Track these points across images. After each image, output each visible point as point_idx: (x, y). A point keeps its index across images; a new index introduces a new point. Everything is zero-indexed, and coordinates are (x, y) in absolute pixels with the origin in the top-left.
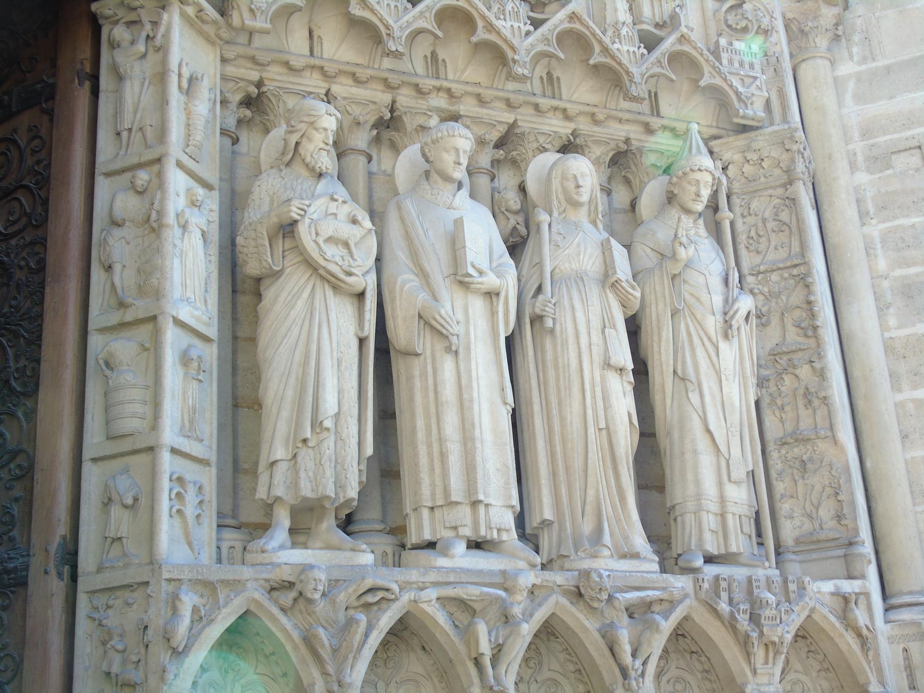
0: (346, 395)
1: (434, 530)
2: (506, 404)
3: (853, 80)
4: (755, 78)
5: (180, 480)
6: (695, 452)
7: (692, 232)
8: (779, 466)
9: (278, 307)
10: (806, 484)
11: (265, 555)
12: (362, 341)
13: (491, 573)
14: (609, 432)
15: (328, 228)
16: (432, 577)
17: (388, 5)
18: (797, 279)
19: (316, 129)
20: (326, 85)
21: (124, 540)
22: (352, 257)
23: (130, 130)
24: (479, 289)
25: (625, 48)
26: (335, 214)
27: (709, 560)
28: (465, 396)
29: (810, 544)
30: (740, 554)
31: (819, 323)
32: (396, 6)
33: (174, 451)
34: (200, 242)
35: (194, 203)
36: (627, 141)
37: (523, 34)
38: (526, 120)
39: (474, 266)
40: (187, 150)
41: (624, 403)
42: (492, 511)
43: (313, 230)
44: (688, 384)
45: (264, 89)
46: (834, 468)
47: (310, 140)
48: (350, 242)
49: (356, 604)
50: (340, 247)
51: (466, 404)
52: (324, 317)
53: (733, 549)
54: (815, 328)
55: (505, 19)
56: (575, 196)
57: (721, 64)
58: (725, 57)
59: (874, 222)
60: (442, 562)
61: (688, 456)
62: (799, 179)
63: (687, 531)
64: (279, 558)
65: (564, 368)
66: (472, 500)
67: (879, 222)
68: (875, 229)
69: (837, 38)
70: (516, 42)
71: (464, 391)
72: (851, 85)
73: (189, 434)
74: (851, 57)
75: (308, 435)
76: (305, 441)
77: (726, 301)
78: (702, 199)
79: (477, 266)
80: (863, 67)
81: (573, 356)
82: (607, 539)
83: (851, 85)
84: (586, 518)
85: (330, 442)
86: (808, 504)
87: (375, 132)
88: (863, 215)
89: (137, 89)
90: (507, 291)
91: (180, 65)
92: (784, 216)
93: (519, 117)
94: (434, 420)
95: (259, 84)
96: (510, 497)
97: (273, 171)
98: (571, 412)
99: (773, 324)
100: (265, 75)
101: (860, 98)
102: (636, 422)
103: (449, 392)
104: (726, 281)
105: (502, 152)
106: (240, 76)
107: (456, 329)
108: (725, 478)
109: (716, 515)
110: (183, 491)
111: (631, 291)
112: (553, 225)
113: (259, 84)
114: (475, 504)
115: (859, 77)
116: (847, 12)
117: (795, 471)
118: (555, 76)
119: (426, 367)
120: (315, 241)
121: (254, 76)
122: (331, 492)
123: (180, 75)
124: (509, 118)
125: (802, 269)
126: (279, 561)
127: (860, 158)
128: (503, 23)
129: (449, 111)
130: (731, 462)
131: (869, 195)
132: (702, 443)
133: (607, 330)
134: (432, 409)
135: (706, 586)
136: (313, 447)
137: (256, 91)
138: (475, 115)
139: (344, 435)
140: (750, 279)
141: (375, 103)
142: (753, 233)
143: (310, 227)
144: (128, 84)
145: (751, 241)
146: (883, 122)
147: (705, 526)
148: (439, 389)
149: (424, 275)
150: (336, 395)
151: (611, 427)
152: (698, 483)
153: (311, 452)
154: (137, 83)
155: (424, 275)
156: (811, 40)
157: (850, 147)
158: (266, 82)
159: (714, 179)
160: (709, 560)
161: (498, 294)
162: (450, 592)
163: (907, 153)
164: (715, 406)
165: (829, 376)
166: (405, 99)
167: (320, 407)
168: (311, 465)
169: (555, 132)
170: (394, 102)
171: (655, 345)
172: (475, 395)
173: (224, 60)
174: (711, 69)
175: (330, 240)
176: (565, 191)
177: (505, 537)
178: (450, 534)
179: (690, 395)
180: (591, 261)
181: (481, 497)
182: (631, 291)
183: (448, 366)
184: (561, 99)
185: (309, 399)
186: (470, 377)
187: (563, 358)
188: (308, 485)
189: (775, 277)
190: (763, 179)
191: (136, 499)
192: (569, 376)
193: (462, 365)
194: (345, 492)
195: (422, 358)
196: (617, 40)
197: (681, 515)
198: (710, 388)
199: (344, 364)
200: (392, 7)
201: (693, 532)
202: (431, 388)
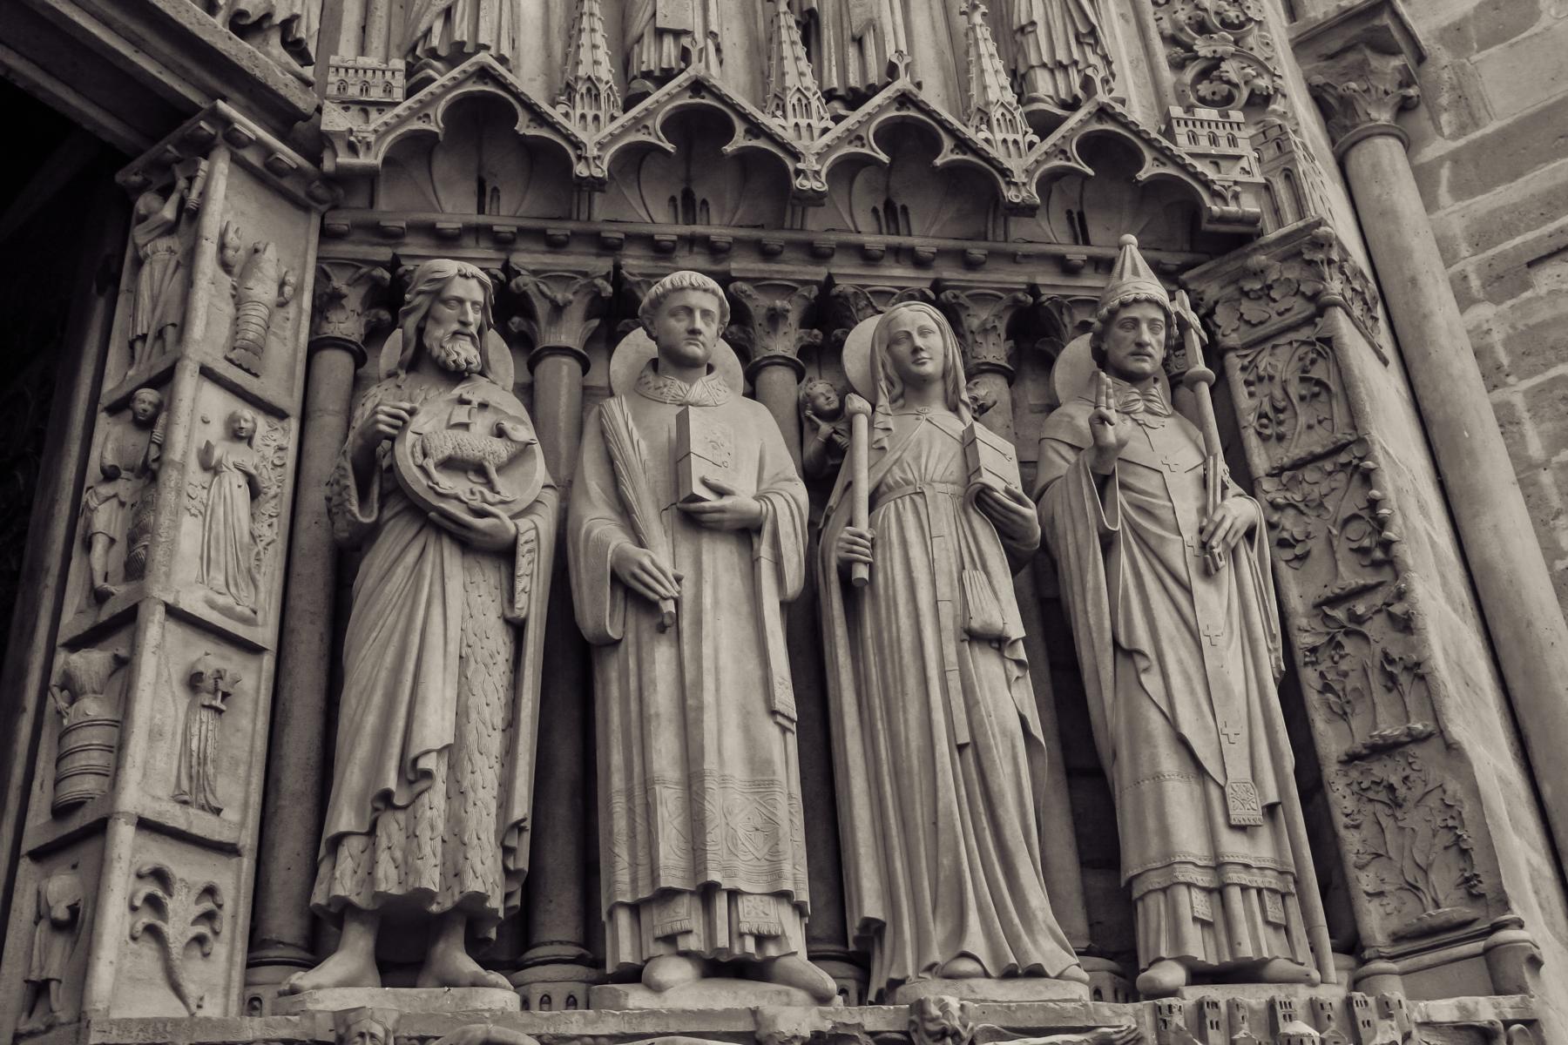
0: (473, 716)
1: (639, 946)
2: (773, 713)
3: (1448, 164)
4: (1239, 158)
5: (160, 876)
6: (1157, 777)
7: (1140, 406)
8: (1349, 804)
9: (370, 583)
10: (1402, 829)
11: (294, 998)
12: (517, 629)
13: (728, 1014)
14: (972, 751)
15: (446, 444)
17: (583, 116)
18: (1349, 470)
19: (445, 302)
20: (503, 256)
21: (53, 985)
22: (493, 489)
23: (144, 337)
25: (999, 136)
26: (466, 426)
27: (1199, 975)
28: (690, 702)
29: (1418, 938)
30: (1264, 963)
31: (1389, 534)
32: (596, 118)
33: (145, 825)
34: (242, 496)
35: (237, 434)
36: (1033, 289)
37: (816, 133)
38: (847, 275)
39: (704, 482)
40: (232, 356)
41: (1009, 699)
42: (744, 905)
43: (418, 448)
44: (1138, 658)
45: (401, 270)
46: (1449, 793)
47: (438, 322)
51: (691, 715)
52: (437, 588)
53: (1247, 950)
54: (1387, 545)
55: (785, 117)
56: (915, 368)
57: (1176, 144)
58: (1181, 134)
59: (1512, 380)
60: (637, 998)
61: (1146, 786)
62: (1335, 304)
63: (1153, 925)
64: (317, 1001)
65: (891, 646)
66: (701, 881)
67: (1521, 379)
68: (1517, 392)
69: (1405, 107)
70: (799, 145)
71: (688, 693)
72: (1445, 173)
73: (186, 798)
74: (1439, 129)
75: (392, 782)
76: (386, 797)
77: (1203, 511)
78: (1150, 349)
79: (712, 479)
80: (1461, 142)
81: (905, 622)
82: (975, 941)
83: (1445, 173)
84: (940, 911)
85: (436, 799)
86: (1408, 864)
87: (596, 322)
88: (1493, 377)
89: (157, 275)
91: (223, 235)
92: (1318, 372)
93: (834, 271)
94: (636, 750)
95: (395, 263)
96: (776, 873)
98: (906, 721)
99: (1315, 552)
100: (402, 251)
101: (1461, 190)
102: (1037, 730)
103: (662, 698)
104: (1204, 482)
105: (816, 331)
106: (360, 256)
108: (1220, 819)
109: (1208, 891)
110: (160, 893)
111: (1014, 505)
112: (879, 418)
113: (395, 263)
114: (707, 893)
115: (1455, 158)
116: (1424, 66)
117: (1379, 806)
118: (898, 206)
119: (627, 661)
120: (421, 467)
121: (384, 253)
122: (431, 879)
123: (222, 247)
124: (819, 273)
125: (1357, 451)
126: (320, 1007)
127: (1475, 283)
128: (782, 121)
130: (1228, 790)
131: (1497, 337)
132: (1169, 762)
133: (966, 574)
134: (635, 732)
135: (1178, 1020)
136: (404, 808)
137: (387, 275)
138: (757, 275)
139: (466, 783)
140: (1267, 485)
141: (585, 274)
142: (1267, 408)
143: (414, 446)
144: (146, 270)
145: (1265, 421)
146: (1506, 218)
147: (1186, 914)
149: (625, 511)
150: (450, 717)
151: (980, 740)
152: (1165, 832)
153: (401, 816)
154: (158, 268)
155: (625, 511)
156: (1360, 113)
157: (1456, 268)
158: (403, 262)
159: (1167, 315)
160: (1199, 975)
161: (759, 531)
163: (1555, 261)
164: (1192, 692)
165: (1420, 625)
166: (634, 263)
168: (398, 838)
169: (901, 288)
170: (617, 268)
171: (1078, 599)
172: (709, 697)
173: (327, 235)
174: (1156, 155)
175: (451, 464)
176: (897, 363)
177: (772, 951)
178: (661, 949)
179: (1143, 678)
180: (941, 467)
181: (714, 876)
182: (1014, 505)
183: (662, 656)
184: (910, 234)
187: (890, 632)
188: (393, 873)
189: (1310, 474)
190: (1275, 317)
191: (74, 910)
192: (901, 658)
194: (462, 883)
195: (622, 647)
196: (984, 127)
197: (1142, 898)
198: (1180, 662)
200: (589, 118)
201: (1163, 924)
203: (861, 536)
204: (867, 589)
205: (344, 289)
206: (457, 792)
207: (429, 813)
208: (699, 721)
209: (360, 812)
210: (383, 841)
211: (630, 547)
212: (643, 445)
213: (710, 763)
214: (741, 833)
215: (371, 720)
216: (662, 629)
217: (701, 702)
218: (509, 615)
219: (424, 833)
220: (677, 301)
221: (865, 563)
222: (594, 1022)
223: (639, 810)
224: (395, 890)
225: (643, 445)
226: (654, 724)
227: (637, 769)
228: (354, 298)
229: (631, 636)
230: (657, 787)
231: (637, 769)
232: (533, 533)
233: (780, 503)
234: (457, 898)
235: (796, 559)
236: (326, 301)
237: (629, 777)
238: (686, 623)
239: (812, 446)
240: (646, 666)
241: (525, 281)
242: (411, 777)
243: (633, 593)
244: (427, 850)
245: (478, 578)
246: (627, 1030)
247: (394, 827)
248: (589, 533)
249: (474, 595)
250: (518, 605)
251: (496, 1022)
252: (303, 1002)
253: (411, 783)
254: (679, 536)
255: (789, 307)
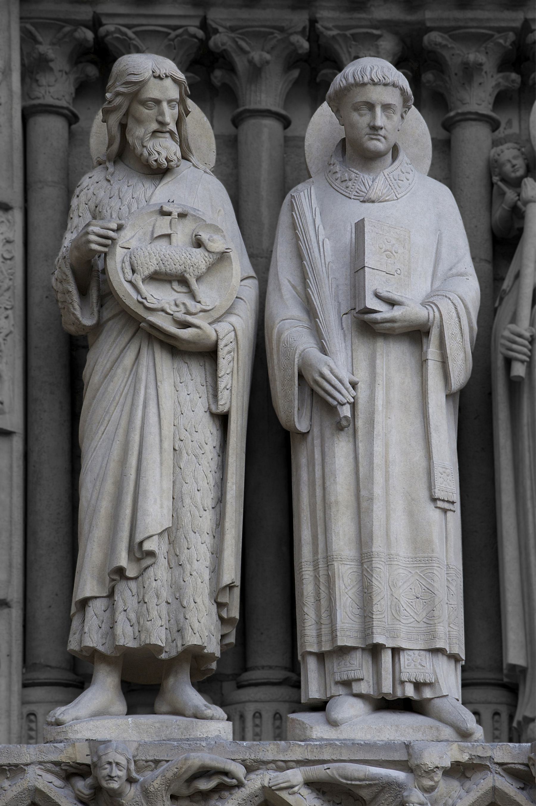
0: (187, 501)
12: (223, 420)
16: (297, 753)
20: (200, 12)
24: (389, 329)
28: (363, 493)
45: (102, 30)
48: (187, 276)
49: (185, 792)
50: (175, 285)
51: (364, 504)
64: (77, 732)
66: (369, 642)
76: (120, 571)
90: (441, 327)
94: (320, 530)
95: (95, 24)
97: (99, 169)
103: (341, 488)
106: (62, 16)
107: (346, 395)
119: (313, 453)
121: (85, 12)
122: (158, 636)
126: (79, 736)
129: (406, 23)
134: (319, 514)
136: (136, 578)
137: (90, 35)
139: (183, 558)
148: (328, 483)
150: (168, 503)
153: (133, 584)
158: (104, 20)
161: (427, 333)
162: (318, 772)
167: (138, 522)
168: (132, 602)
172: (378, 490)
181: (379, 639)
185: (127, 511)
186: (371, 463)
188: (129, 630)
193: (361, 446)
195: (310, 437)
199: (185, 456)
202: (318, 482)
203: (520, 336)
204: (526, 381)
205: (51, 54)
206: (176, 563)
207: (154, 584)
208: (370, 510)
209: (101, 581)
210: (120, 605)
211: (314, 353)
212: (328, 244)
213: (378, 546)
214: (403, 601)
215: (105, 506)
216: (340, 428)
217: (372, 494)
218: (214, 410)
219: (152, 601)
220: (360, 96)
221: (523, 362)
222: (285, 751)
223: (322, 579)
224: (131, 644)
225: (328, 244)
226: (334, 510)
227: (321, 546)
228: (59, 61)
229: (316, 431)
230: (336, 564)
231: (321, 546)
232: (232, 334)
233: (446, 307)
234: (180, 649)
235: (462, 355)
236: (33, 68)
237: (315, 552)
238: (360, 423)
239: (498, 213)
240: (327, 459)
241: (221, 40)
242: (138, 555)
243: (315, 394)
244: (154, 614)
245: (187, 378)
246: (310, 757)
247: (128, 593)
248: (280, 334)
249: (183, 394)
250: (221, 402)
251: (211, 749)
252: (65, 732)
253: (139, 560)
254: (356, 341)
255: (482, 58)
